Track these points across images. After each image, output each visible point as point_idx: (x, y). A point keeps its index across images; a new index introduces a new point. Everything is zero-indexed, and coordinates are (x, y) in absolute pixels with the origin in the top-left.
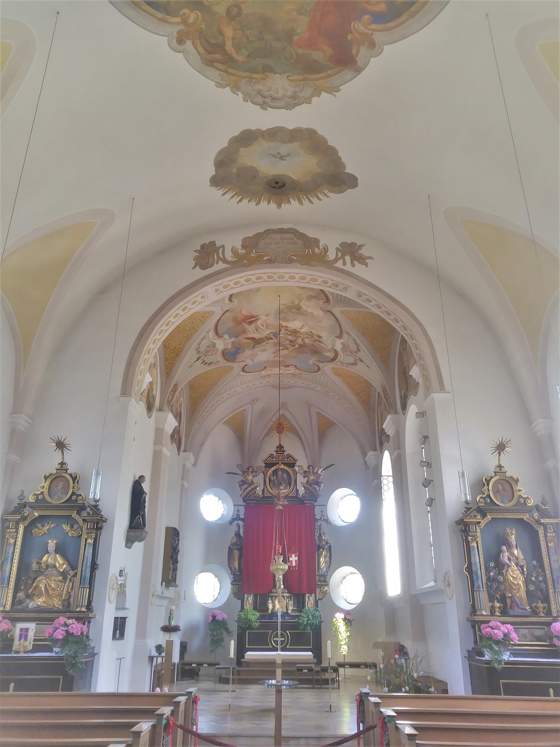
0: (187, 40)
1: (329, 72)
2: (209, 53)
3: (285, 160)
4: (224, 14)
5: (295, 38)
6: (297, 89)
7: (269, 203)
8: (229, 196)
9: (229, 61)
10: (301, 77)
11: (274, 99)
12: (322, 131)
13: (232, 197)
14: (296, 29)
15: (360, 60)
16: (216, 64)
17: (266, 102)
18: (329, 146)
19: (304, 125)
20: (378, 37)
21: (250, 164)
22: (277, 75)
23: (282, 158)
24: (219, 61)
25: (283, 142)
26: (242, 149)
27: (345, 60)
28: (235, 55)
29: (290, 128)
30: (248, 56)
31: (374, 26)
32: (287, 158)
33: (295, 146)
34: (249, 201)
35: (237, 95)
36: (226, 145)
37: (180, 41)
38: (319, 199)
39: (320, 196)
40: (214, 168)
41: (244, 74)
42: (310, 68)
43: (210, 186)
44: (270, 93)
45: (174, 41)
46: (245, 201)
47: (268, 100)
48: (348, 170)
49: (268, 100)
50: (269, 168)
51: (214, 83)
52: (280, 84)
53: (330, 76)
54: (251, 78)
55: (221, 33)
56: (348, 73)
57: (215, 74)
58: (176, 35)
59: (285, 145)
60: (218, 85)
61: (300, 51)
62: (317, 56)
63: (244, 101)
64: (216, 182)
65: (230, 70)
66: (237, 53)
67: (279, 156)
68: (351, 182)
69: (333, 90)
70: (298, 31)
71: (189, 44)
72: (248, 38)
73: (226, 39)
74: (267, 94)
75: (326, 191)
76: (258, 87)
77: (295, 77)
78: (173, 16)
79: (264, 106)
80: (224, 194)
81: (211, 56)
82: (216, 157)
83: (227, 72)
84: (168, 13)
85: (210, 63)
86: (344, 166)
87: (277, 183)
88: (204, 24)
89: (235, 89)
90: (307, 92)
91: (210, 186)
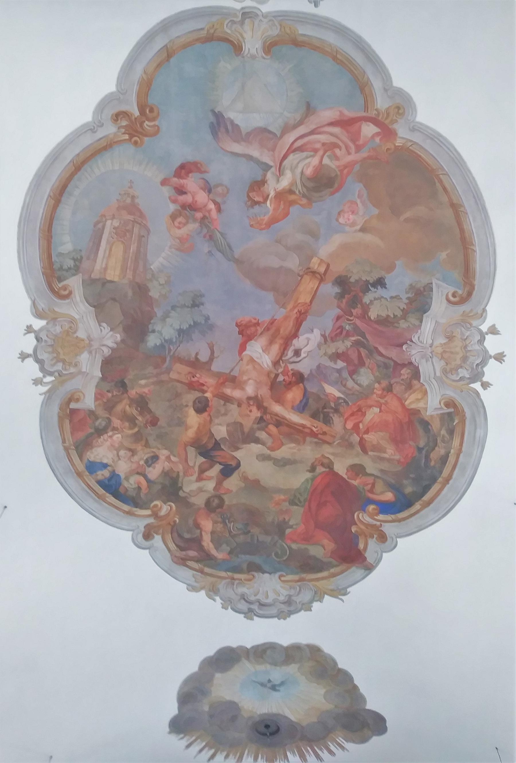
0: (155, 535)
1: (332, 570)
2: (182, 549)
3: (279, 691)
4: (203, 506)
5: (288, 531)
6: (292, 592)
7: (256, 759)
8: (195, 748)
9: (206, 558)
10: (296, 577)
11: (262, 605)
12: (327, 649)
13: (201, 751)
14: (289, 520)
16: (189, 563)
17: (253, 608)
18: (340, 671)
19: (303, 640)
20: (388, 529)
21: (228, 698)
22: (266, 575)
23: (274, 688)
24: (192, 559)
25: (275, 664)
26: (218, 675)
27: (352, 556)
28: (214, 552)
30: (230, 553)
31: (381, 517)
32: (282, 689)
33: (292, 669)
34: (226, 757)
35: (214, 600)
36: (195, 668)
37: (147, 536)
38: (331, 752)
39: (332, 748)
41: (223, 574)
42: (309, 566)
44: (257, 597)
45: (140, 536)
46: (220, 758)
47: (255, 607)
49: (255, 607)
50: (257, 705)
51: (185, 586)
52: (270, 586)
53: (334, 575)
54: (233, 579)
55: (197, 526)
56: (356, 572)
57: (187, 573)
58: (143, 529)
59: (278, 668)
60: (190, 588)
61: (294, 546)
62: (316, 551)
63: (222, 608)
64: (178, 726)
65: (207, 570)
66: (217, 549)
67: (269, 685)
69: (339, 593)
70: (291, 523)
71: (157, 540)
72: (230, 532)
73: (203, 533)
74: (252, 598)
75: (340, 740)
76: (241, 590)
77: (290, 577)
78: (141, 508)
79: (249, 614)
80: (188, 746)
81: (184, 553)
82: (181, 688)
83: (202, 572)
84: (137, 505)
85: (182, 561)
86: (362, 699)
87: (267, 726)
88: (177, 516)
89: (211, 593)
90: (306, 596)
91: (170, 733)
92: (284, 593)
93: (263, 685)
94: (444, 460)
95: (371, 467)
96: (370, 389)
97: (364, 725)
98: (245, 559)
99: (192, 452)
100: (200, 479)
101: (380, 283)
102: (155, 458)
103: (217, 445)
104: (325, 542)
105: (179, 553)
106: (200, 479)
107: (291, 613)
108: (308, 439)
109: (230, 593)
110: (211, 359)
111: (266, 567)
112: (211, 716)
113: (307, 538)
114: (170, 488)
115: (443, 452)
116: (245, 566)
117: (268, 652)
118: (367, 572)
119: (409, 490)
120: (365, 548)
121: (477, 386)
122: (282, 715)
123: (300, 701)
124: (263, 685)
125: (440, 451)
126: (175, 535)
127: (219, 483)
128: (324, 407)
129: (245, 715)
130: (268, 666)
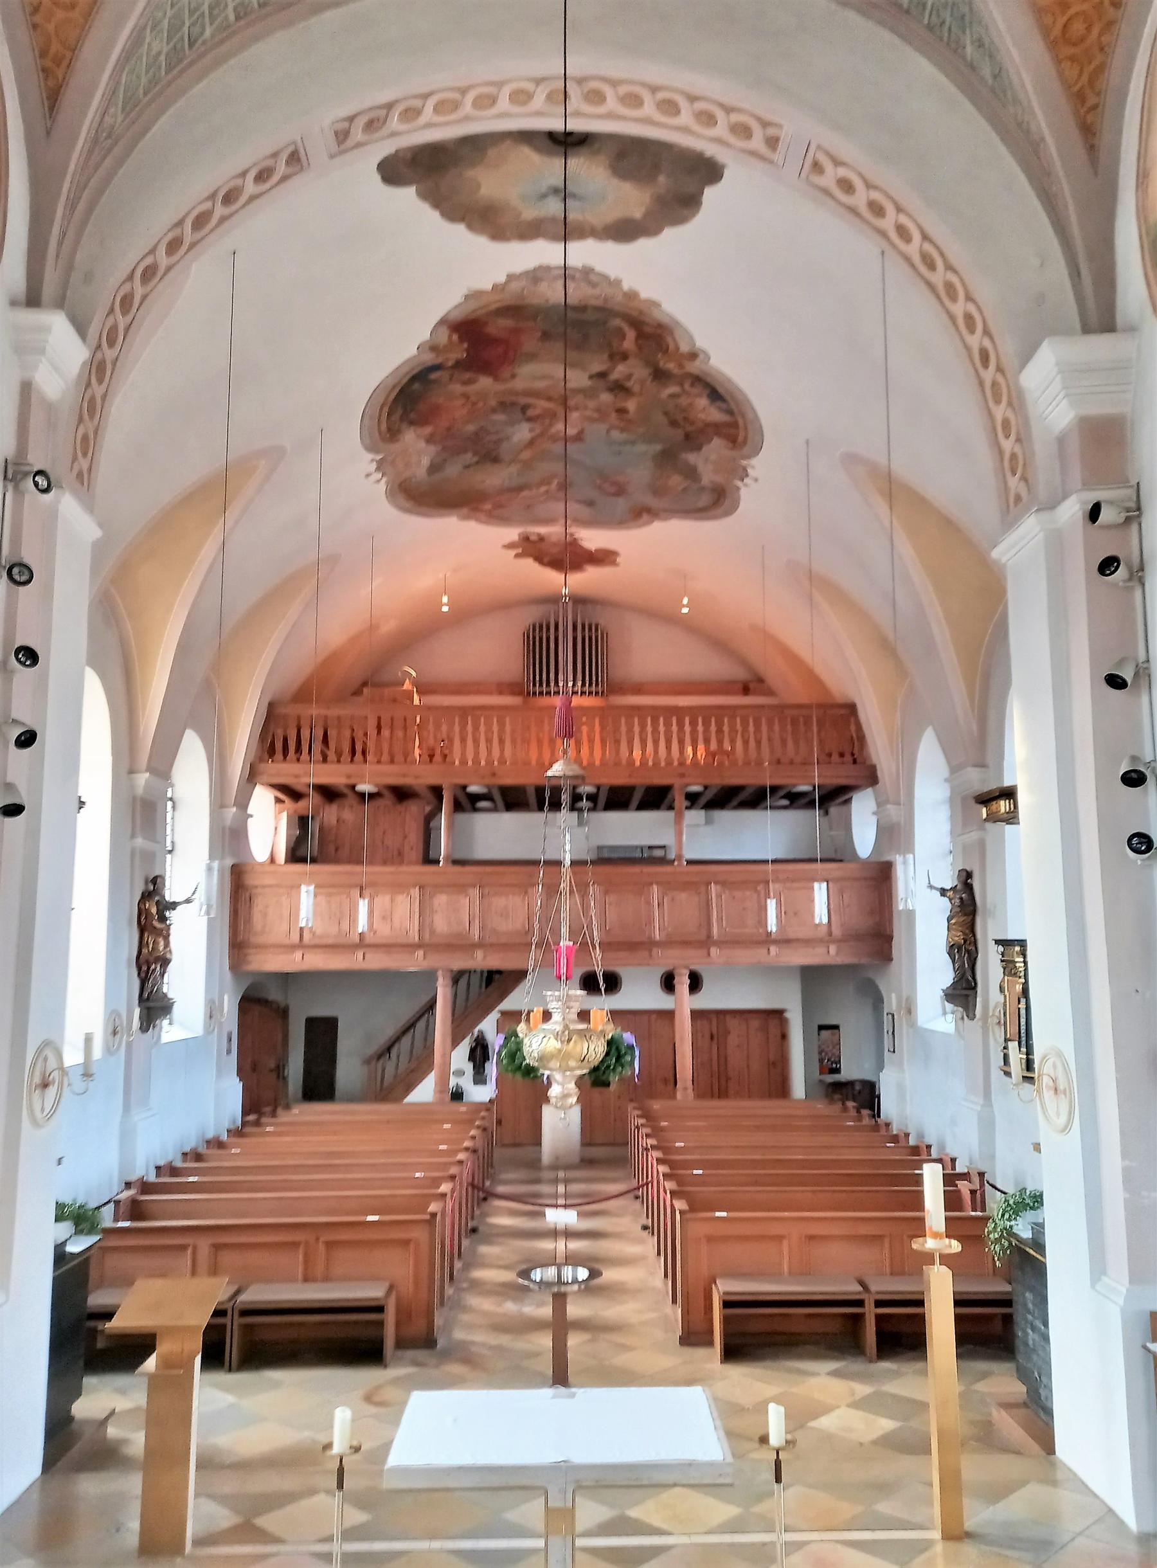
15: (443, 337)
32: (544, 190)
33: (530, 213)
48: (410, 192)
56: (457, 316)
62: (505, 323)
68: (393, 171)
76: (597, 291)
82: (694, 216)
85: (660, 326)
86: (423, 195)
90: (515, 286)
92: (543, 287)
95: (458, 388)
98: (590, 316)
99: (636, 388)
101: (467, 467)
102: (672, 396)
107: (535, 270)
110: (608, 431)
113: (516, 331)
114: (660, 375)
119: (416, 386)
120: (450, 337)
125: (396, 417)
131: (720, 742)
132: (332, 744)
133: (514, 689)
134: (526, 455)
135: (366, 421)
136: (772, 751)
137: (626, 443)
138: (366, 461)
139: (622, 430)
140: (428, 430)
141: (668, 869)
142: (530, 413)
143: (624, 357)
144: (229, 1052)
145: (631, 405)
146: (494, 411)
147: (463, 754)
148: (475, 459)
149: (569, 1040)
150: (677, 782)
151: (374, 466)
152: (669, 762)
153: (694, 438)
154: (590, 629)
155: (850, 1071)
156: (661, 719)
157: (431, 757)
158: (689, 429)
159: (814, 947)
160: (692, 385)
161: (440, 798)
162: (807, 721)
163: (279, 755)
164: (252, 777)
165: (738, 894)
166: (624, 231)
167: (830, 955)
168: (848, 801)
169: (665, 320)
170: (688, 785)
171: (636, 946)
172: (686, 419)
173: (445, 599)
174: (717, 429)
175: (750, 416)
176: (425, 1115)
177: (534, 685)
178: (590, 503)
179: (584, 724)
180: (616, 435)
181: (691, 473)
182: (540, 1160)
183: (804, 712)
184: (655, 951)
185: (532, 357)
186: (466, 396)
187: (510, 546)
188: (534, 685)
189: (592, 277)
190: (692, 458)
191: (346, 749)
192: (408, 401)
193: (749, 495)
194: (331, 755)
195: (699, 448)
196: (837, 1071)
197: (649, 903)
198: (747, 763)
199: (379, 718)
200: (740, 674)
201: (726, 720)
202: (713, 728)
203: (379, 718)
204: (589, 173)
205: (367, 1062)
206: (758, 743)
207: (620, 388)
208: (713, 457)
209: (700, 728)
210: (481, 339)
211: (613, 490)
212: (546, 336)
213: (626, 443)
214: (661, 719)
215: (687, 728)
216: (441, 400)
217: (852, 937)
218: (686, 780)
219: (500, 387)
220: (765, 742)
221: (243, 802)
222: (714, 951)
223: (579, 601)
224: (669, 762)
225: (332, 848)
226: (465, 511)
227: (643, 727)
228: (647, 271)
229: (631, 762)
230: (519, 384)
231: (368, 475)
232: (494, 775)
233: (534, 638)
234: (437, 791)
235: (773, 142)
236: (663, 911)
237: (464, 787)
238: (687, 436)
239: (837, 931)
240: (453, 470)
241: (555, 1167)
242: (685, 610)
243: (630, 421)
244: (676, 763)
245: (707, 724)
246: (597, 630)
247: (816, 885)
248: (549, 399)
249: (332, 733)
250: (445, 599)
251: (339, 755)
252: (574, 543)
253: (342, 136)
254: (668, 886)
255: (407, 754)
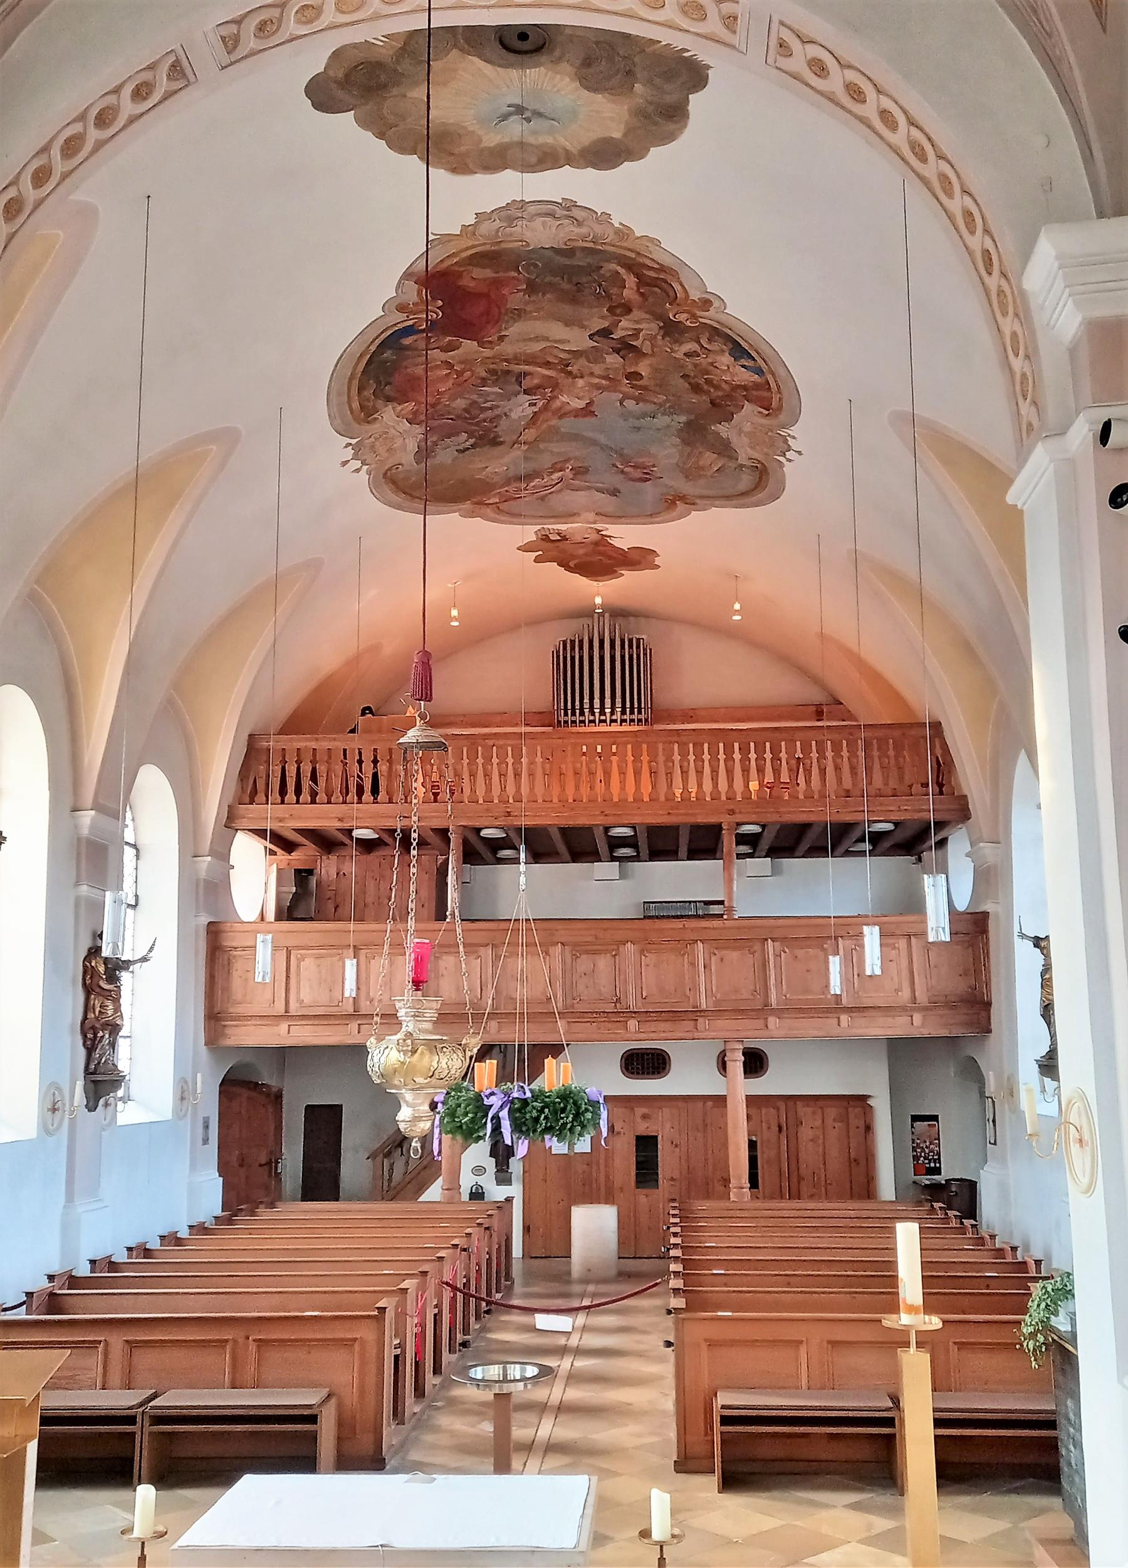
9: (632, 266)
10: (504, 246)
11: (552, 215)
15: (412, 292)
16: (656, 266)
23: (519, 110)
25: (522, 144)
26: (617, 135)
29: (508, 172)
31: (411, 323)
33: (492, 139)
40: (690, 107)
43: (709, 67)
47: (560, 212)
49: (560, 212)
52: (541, 235)
65: (633, 255)
67: (527, 114)
68: (324, 95)
76: (584, 230)
79: (569, 206)
85: (662, 269)
86: (364, 123)
90: (486, 228)
91: (709, 67)
93: (539, 114)
94: (360, 390)
95: (435, 354)
96: (453, 398)
97: (346, 82)
98: (580, 261)
99: (646, 348)
100: (639, 331)
103: (617, 351)
104: (472, 284)
105: (669, 278)
106: (639, 331)
108: (511, 357)
109: (598, 229)
111: (549, 253)
112: (629, 73)
113: (497, 283)
114: (671, 329)
115: (366, 393)
116: (578, 254)
117: (533, 160)
118: (411, 270)
120: (419, 293)
121: (354, 441)
122: (499, 66)
123: (471, 93)
124: (539, 114)
125: (368, 393)
126: (672, 294)
127: (616, 324)
128: (497, 380)
129: (565, 66)
130: (531, 140)
131: (777, 772)
132: (322, 782)
133: (545, 718)
134: (530, 435)
135: (333, 396)
136: (840, 780)
137: (644, 415)
138: (339, 447)
139: (638, 400)
140: (410, 406)
141: (716, 923)
142: (527, 383)
143: (628, 310)
144: (206, 1141)
145: (643, 368)
146: (484, 382)
147: (473, 791)
148: (472, 441)
149: (414, 1052)
150: (726, 820)
151: (350, 452)
152: (715, 796)
153: (723, 405)
154: (631, 646)
155: (949, 1170)
156: (706, 746)
157: (436, 795)
158: (715, 393)
159: (894, 1017)
160: (710, 340)
161: (448, 841)
162: (882, 743)
163: (261, 797)
164: (230, 822)
165: (800, 953)
166: (604, 155)
167: (918, 1025)
168: (942, 843)
169: (666, 261)
170: (739, 824)
171: (683, 1017)
172: (708, 381)
173: (454, 613)
174: (748, 393)
175: (781, 372)
176: (432, 1216)
177: (566, 714)
178: (615, 492)
179: (614, 754)
180: (630, 404)
181: (725, 449)
182: (569, 1273)
183: (880, 733)
184: (700, 1020)
185: (519, 314)
186: (449, 365)
187: (526, 548)
188: (566, 714)
189: (576, 213)
190: (723, 429)
191: (337, 783)
192: (380, 373)
193: (793, 471)
194: (321, 796)
195: (729, 418)
196: (937, 1171)
197: (693, 964)
198: (809, 796)
199: (375, 750)
200: (815, 695)
201: (783, 743)
202: (768, 756)
203: (375, 750)
204: (551, 84)
205: (372, 1156)
206: (823, 771)
207: (625, 348)
208: (748, 427)
209: (753, 756)
210: (458, 294)
211: (638, 474)
212: (532, 288)
213: (644, 415)
214: (706, 746)
215: (737, 756)
216: (420, 370)
217: (939, 1004)
218: (739, 818)
219: (487, 352)
220: (830, 770)
221: (222, 854)
222: (772, 1021)
223: (618, 613)
224: (715, 796)
225: (331, 907)
226: (467, 505)
227: (684, 755)
228: (640, 201)
229: (670, 798)
230: (508, 348)
231: (345, 463)
232: (509, 814)
233: (565, 658)
234: (443, 833)
235: (730, 21)
236: (709, 975)
237: (479, 830)
238: (712, 403)
239: (922, 997)
240: (445, 456)
241: (585, 1281)
242: (737, 618)
243: (645, 388)
244: (724, 798)
245: (760, 751)
246: (638, 647)
247: (866, 929)
248: (547, 364)
249: (321, 769)
250: (454, 613)
251: (329, 795)
252: (602, 541)
253: (231, 43)
254: (718, 943)
255: (407, 794)
